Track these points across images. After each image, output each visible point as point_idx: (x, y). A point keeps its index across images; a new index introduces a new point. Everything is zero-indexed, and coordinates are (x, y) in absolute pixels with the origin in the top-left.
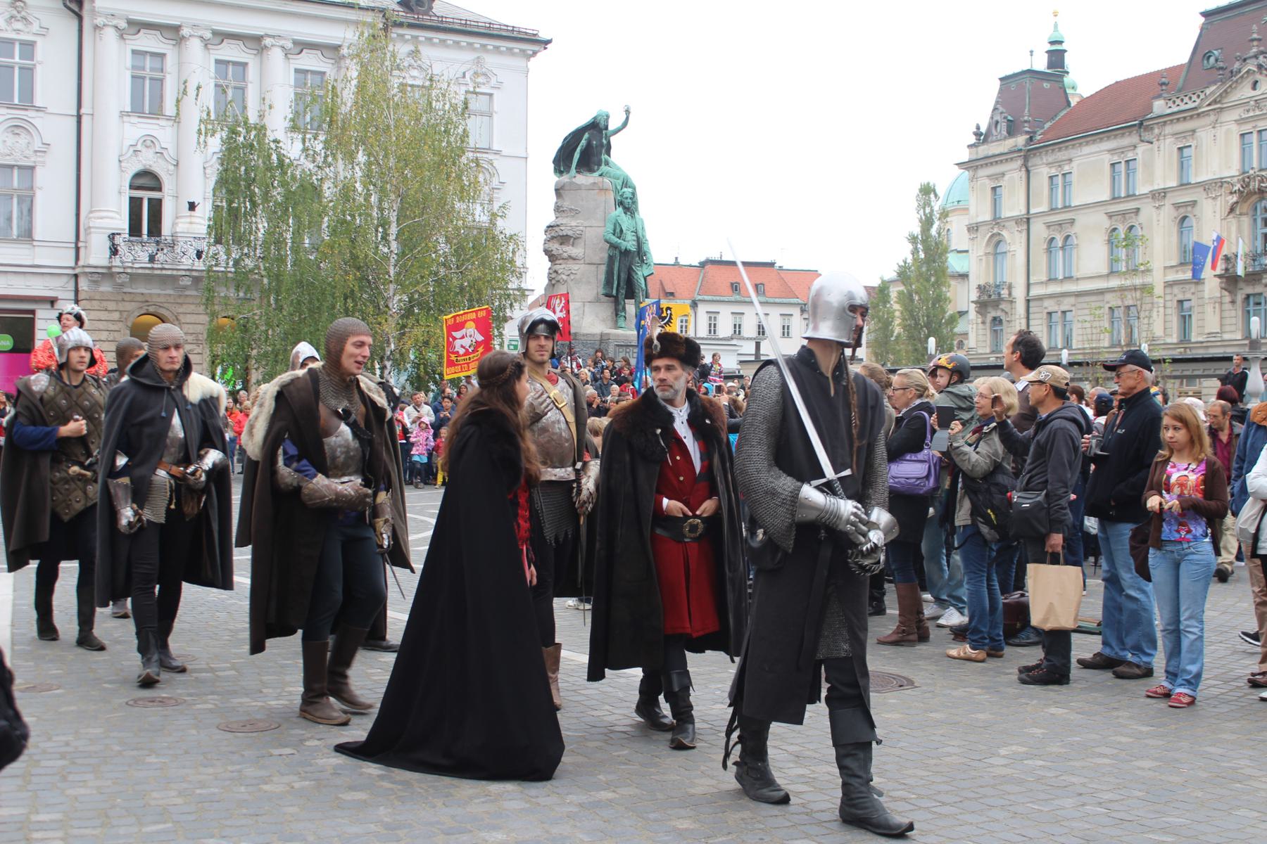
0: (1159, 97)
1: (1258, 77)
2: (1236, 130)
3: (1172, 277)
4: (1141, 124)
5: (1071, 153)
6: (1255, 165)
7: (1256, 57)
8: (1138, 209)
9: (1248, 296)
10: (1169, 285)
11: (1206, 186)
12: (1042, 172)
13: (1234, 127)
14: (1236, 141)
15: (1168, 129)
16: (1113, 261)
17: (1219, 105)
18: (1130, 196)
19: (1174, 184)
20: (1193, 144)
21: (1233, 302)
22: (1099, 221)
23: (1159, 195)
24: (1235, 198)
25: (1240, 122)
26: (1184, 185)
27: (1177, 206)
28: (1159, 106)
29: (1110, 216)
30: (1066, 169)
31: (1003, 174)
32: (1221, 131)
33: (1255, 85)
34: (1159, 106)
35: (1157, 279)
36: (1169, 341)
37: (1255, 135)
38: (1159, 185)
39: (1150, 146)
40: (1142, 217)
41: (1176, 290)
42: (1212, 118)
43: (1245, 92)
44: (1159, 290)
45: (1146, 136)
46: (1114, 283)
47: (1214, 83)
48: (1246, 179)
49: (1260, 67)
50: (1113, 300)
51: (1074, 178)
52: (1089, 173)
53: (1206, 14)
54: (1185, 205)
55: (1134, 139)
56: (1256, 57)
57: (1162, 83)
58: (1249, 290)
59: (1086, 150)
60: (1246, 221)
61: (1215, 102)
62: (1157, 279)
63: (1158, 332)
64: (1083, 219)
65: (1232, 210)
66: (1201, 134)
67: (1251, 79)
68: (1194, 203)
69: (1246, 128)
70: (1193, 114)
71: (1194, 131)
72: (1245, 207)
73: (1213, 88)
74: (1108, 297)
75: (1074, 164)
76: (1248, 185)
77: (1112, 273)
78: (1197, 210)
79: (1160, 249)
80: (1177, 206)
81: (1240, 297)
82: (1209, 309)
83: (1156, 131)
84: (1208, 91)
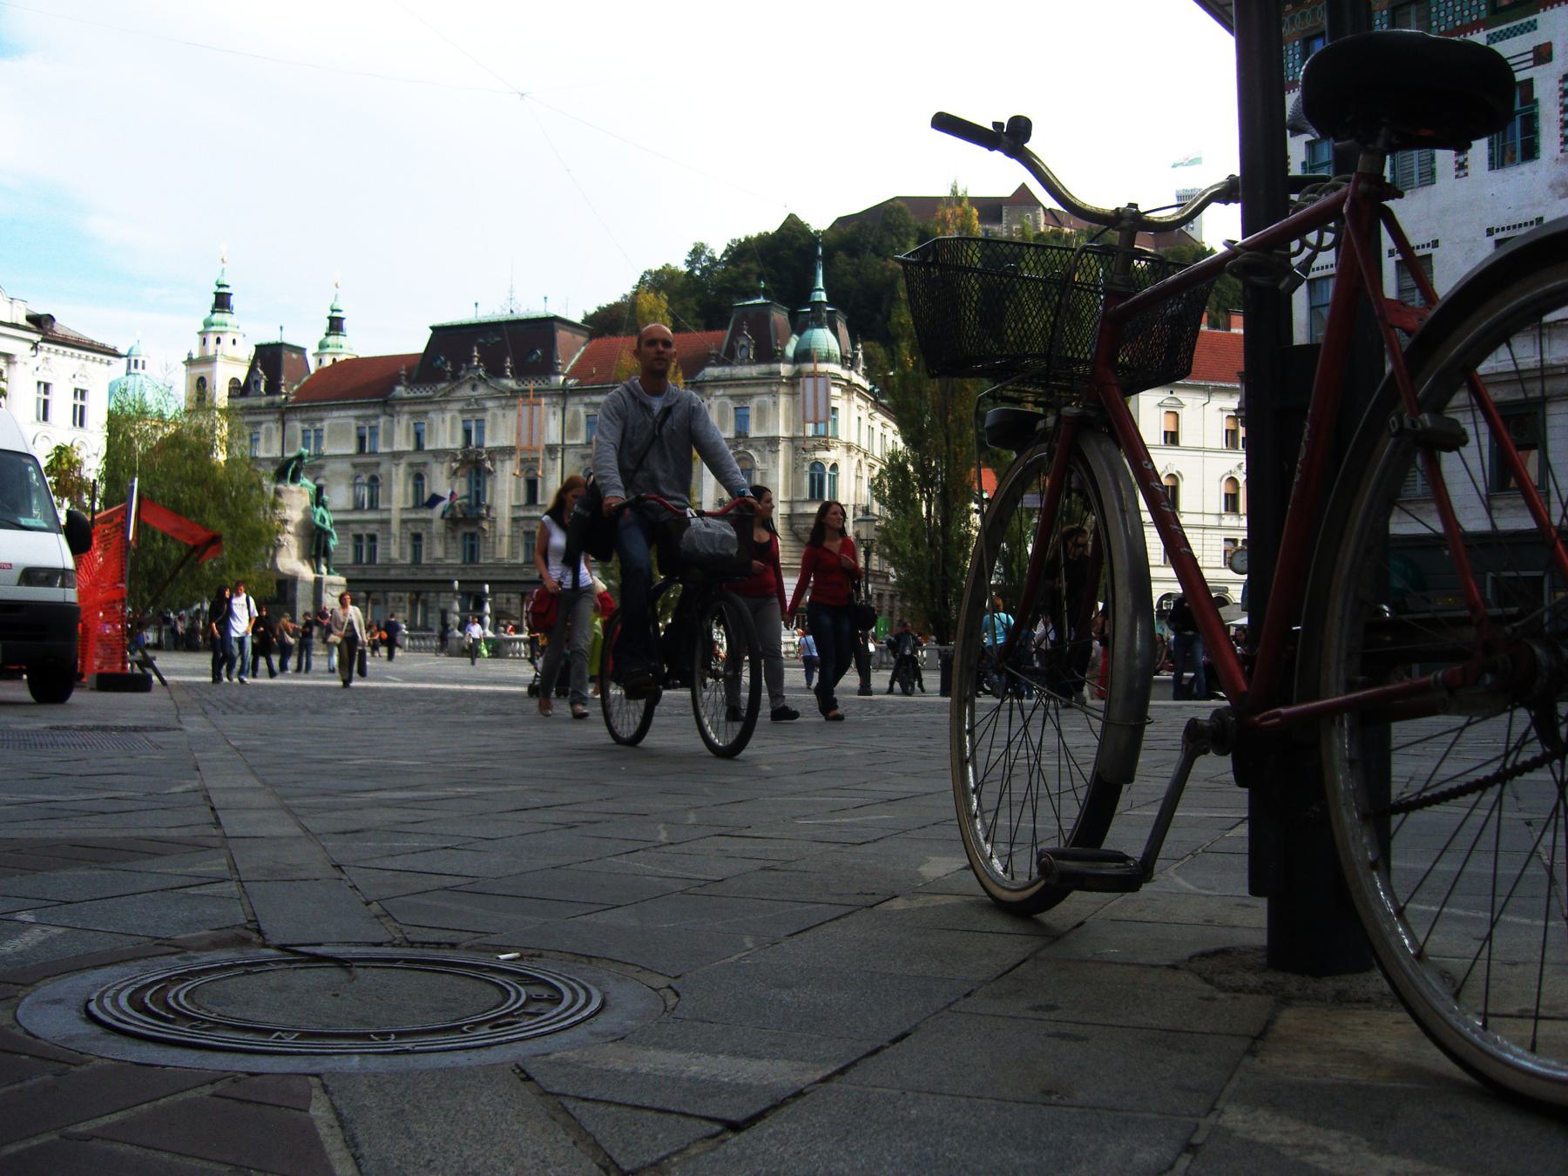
3: (405, 516)
5: (324, 414)
8: (378, 465)
9: (465, 535)
12: (296, 426)
15: (406, 408)
16: (356, 498)
17: (447, 399)
18: (373, 453)
19: (411, 448)
21: (454, 538)
22: (345, 466)
23: (396, 456)
25: (462, 411)
29: (355, 466)
30: (318, 425)
31: (260, 423)
32: (448, 416)
35: (396, 517)
40: (382, 470)
43: (466, 391)
44: (395, 527)
45: (388, 410)
46: (357, 516)
50: (357, 529)
51: (325, 434)
52: (338, 434)
55: (377, 411)
58: (467, 530)
59: (336, 414)
62: (396, 517)
63: (394, 552)
64: (331, 467)
66: (432, 415)
68: (425, 464)
70: (428, 400)
74: (352, 526)
75: (326, 424)
77: (358, 507)
78: (427, 470)
79: (399, 493)
80: (411, 465)
81: (460, 534)
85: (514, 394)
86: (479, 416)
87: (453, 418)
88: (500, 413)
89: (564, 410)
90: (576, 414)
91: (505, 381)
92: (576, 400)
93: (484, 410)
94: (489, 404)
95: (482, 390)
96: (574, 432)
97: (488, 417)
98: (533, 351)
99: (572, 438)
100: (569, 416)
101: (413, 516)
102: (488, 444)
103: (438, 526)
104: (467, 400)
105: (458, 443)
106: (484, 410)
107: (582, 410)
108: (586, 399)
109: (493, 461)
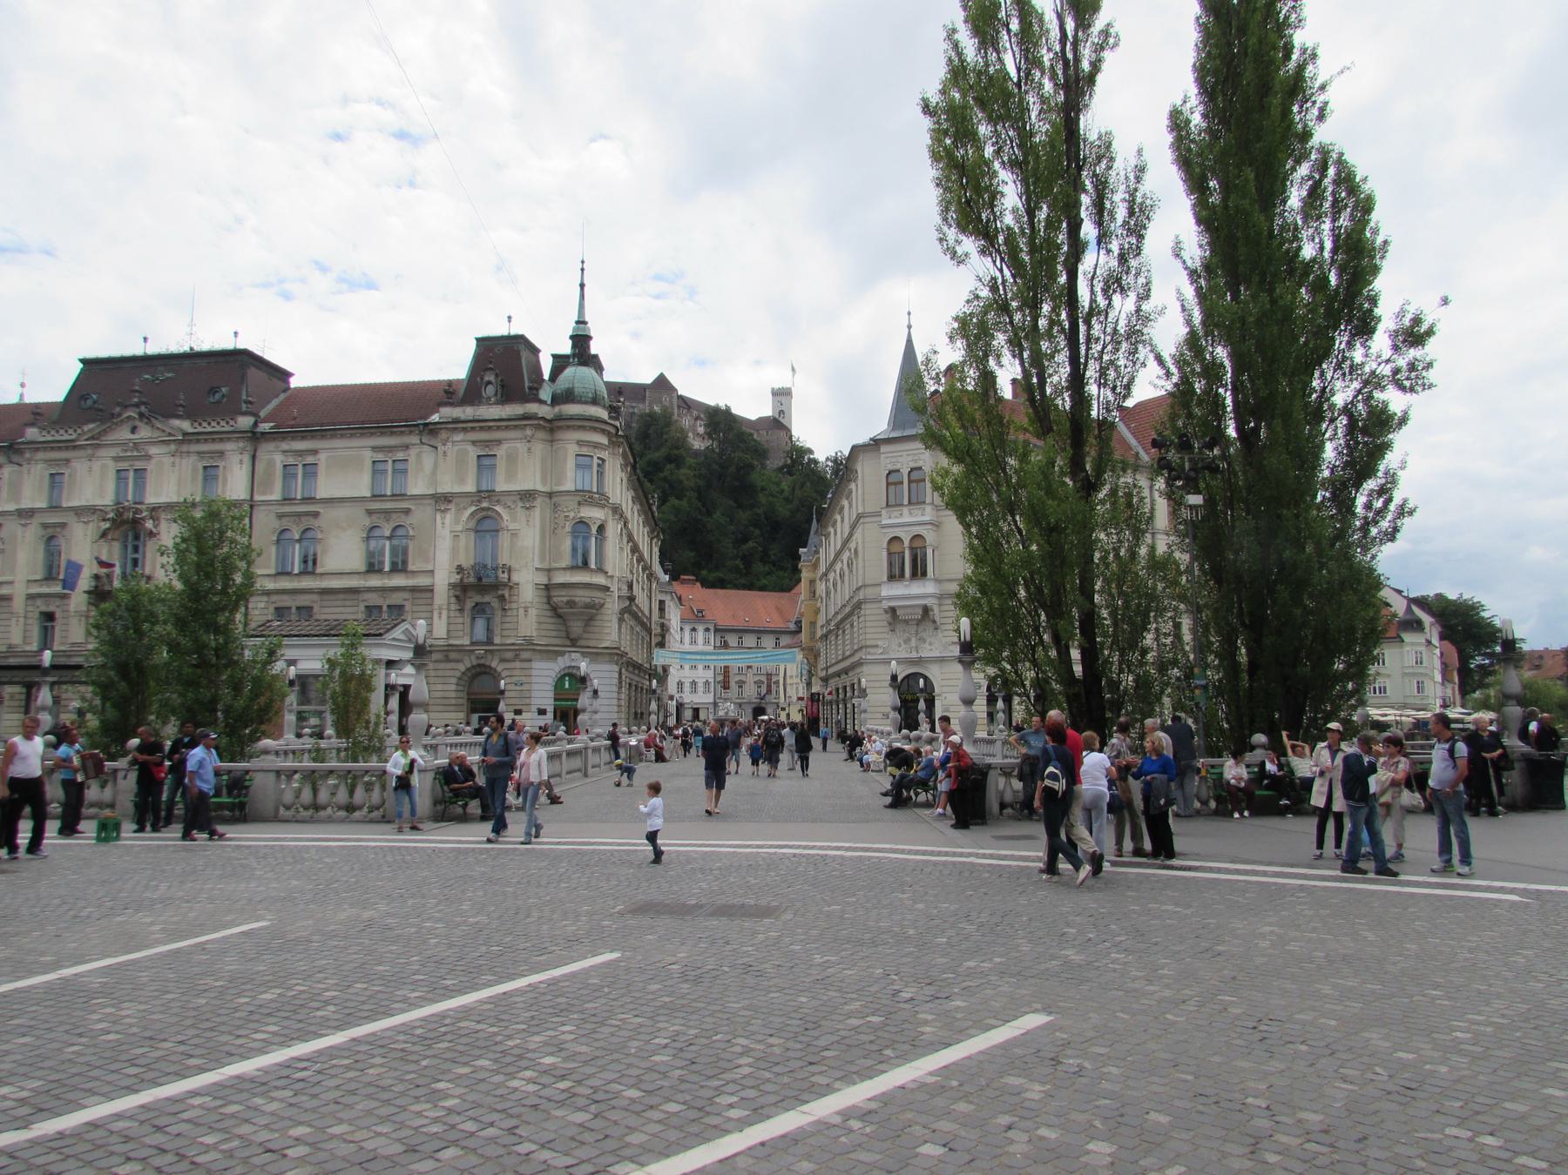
0: (32, 425)
1: (137, 423)
2: (112, 467)
3: (35, 590)
4: (10, 447)
6: (130, 497)
7: (137, 405)
10: (31, 597)
11: (78, 511)
13: (111, 463)
14: (112, 475)
15: (40, 455)
17: (96, 441)
19: (42, 504)
20: (67, 471)
24: (108, 525)
25: (117, 459)
26: (54, 508)
27: (45, 526)
28: (32, 433)
32: (96, 465)
33: (134, 430)
34: (32, 433)
36: (28, 648)
37: (131, 474)
38: (26, 504)
39: (16, 468)
41: (39, 602)
42: (90, 451)
43: (124, 434)
44: (19, 604)
45: (16, 458)
47: (93, 421)
48: (120, 510)
49: (141, 415)
53: (83, 361)
54: (55, 525)
56: (137, 405)
57: (37, 414)
60: (117, 546)
61: (93, 438)
65: (104, 535)
66: (76, 465)
67: (130, 424)
68: (63, 525)
69: (124, 465)
70: (70, 446)
71: (68, 461)
72: (117, 534)
73: (91, 426)
76: (121, 514)
82: (74, 621)
83: (28, 455)
84: (86, 428)
85: (188, 438)
86: (139, 465)
87: (104, 466)
88: (167, 460)
89: (254, 457)
90: (271, 463)
91: (176, 423)
92: (270, 446)
93: (148, 457)
94: (153, 450)
95: (145, 432)
96: (268, 487)
97: (151, 466)
98: (213, 390)
99: (264, 493)
100: (260, 467)
101: (45, 590)
102: (152, 498)
103: (79, 599)
104: (123, 444)
105: (107, 499)
106: (148, 457)
107: (279, 459)
108: (285, 446)
109: (156, 519)
